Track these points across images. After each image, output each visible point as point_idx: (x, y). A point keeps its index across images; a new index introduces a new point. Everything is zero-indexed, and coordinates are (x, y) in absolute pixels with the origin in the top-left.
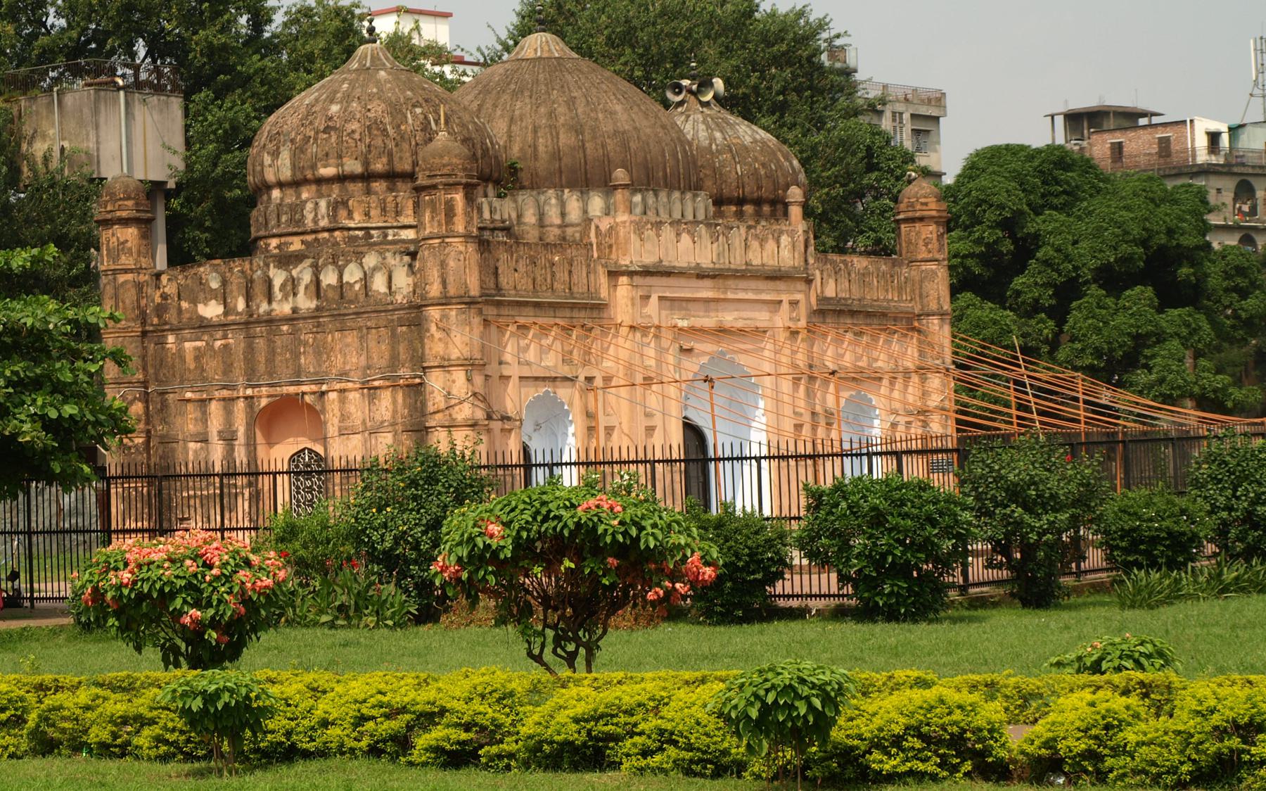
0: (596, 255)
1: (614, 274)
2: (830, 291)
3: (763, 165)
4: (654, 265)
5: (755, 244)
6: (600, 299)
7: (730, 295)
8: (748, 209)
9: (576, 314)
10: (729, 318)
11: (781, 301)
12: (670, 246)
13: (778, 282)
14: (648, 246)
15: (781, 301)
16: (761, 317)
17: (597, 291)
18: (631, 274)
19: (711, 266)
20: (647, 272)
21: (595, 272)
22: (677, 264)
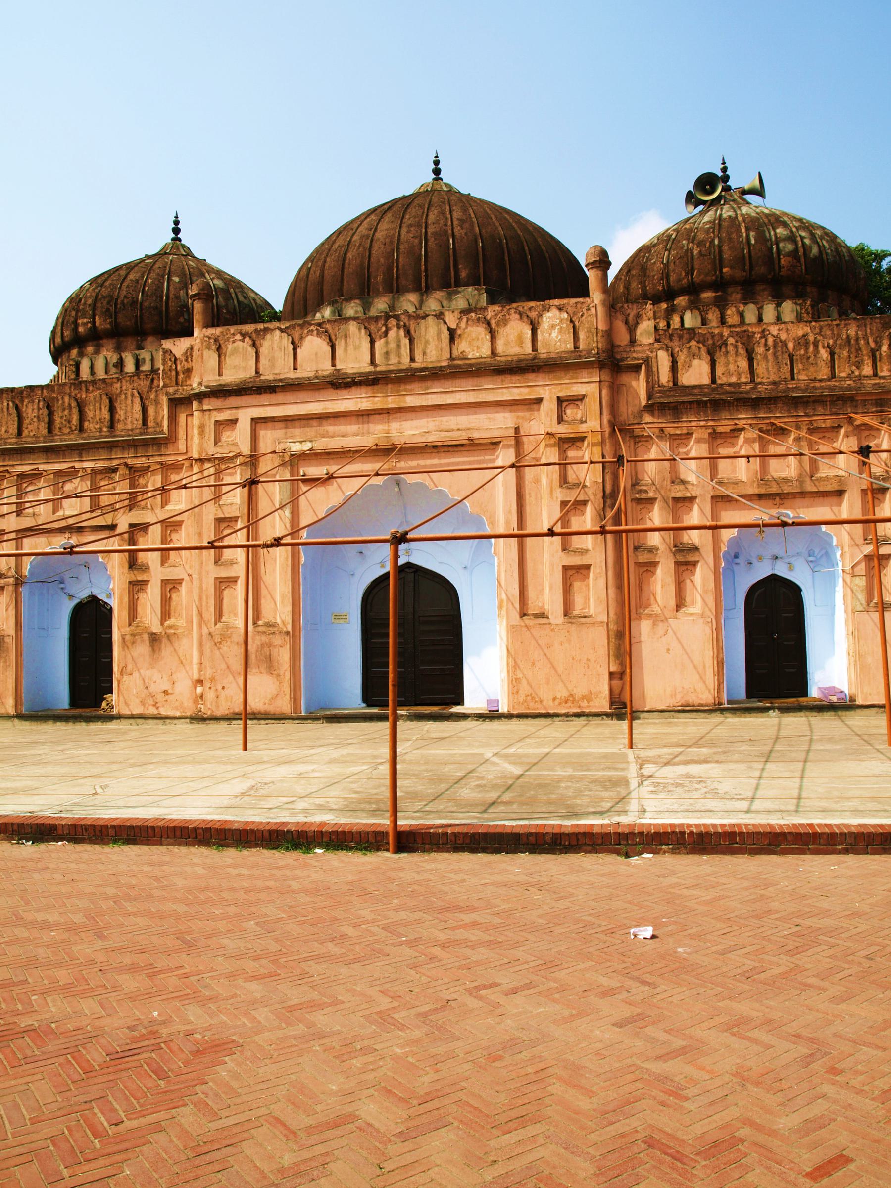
0: (162, 384)
1: (178, 404)
2: (696, 373)
3: (700, 244)
4: (245, 382)
5: (479, 332)
6: (162, 432)
7: (411, 401)
8: (681, 301)
9: (117, 454)
10: (409, 431)
11: (539, 401)
12: (279, 355)
13: (531, 376)
14: (230, 361)
15: (539, 401)
16: (498, 424)
17: (159, 424)
18: (200, 396)
19: (372, 369)
20: (221, 392)
21: (157, 403)
22: (292, 375)
